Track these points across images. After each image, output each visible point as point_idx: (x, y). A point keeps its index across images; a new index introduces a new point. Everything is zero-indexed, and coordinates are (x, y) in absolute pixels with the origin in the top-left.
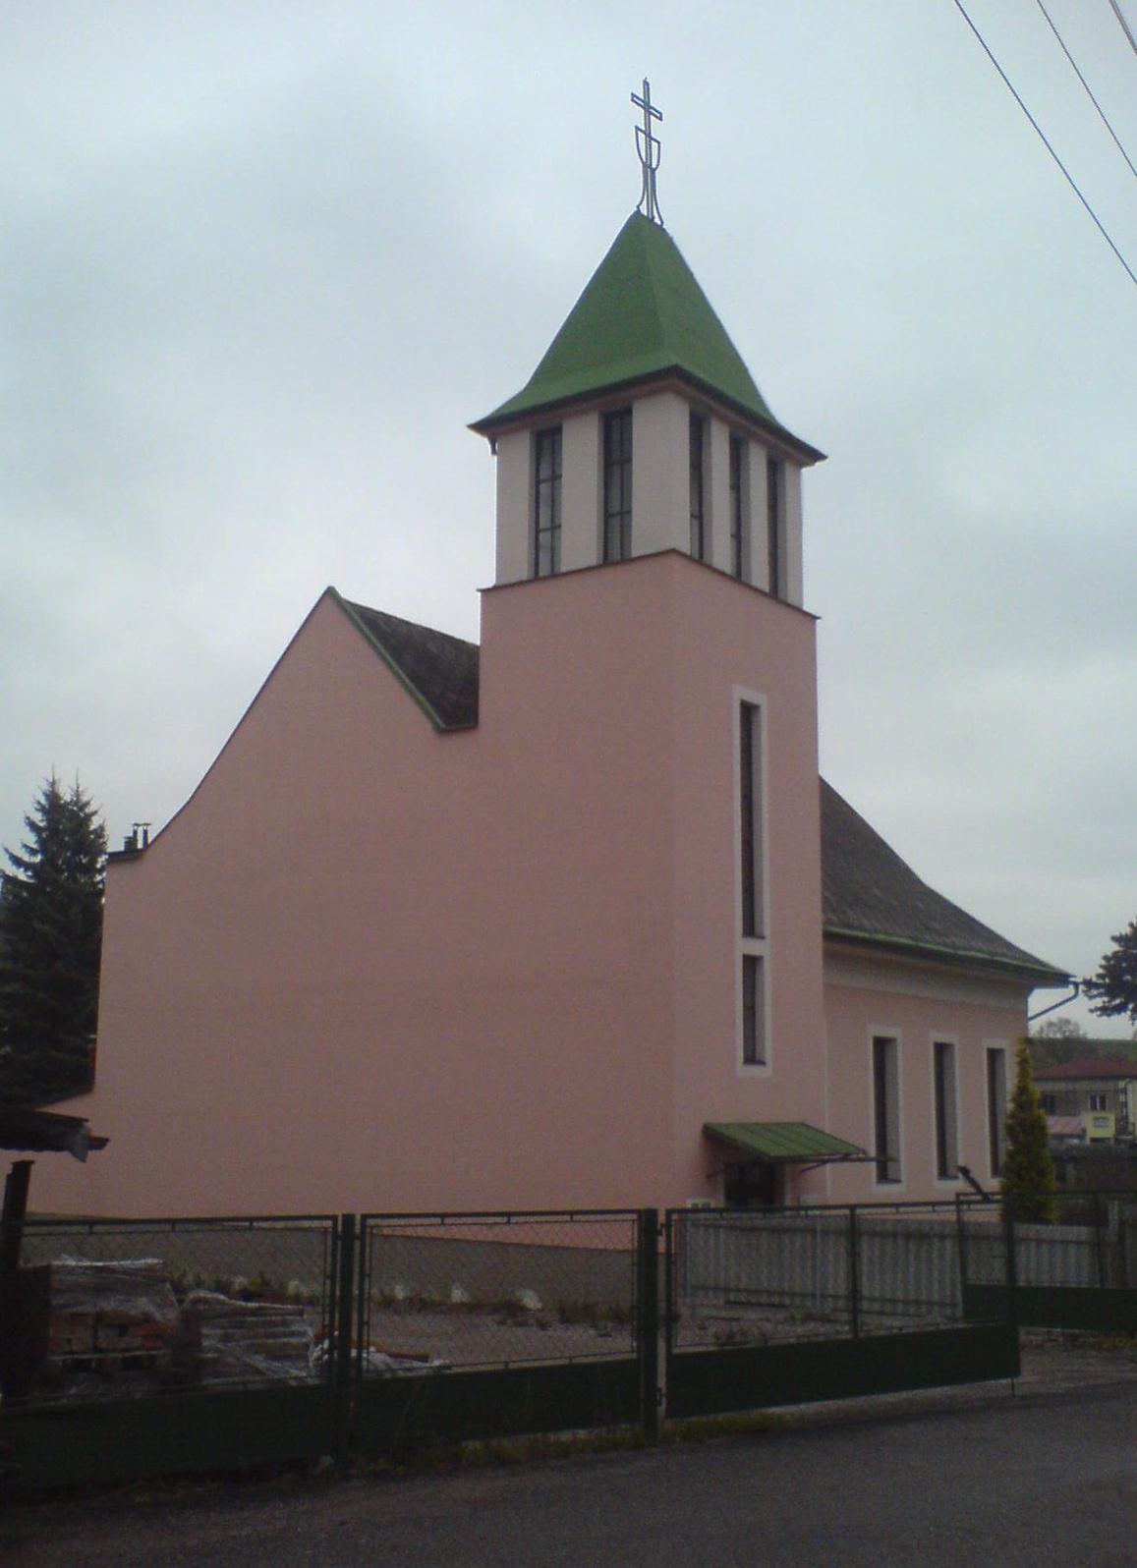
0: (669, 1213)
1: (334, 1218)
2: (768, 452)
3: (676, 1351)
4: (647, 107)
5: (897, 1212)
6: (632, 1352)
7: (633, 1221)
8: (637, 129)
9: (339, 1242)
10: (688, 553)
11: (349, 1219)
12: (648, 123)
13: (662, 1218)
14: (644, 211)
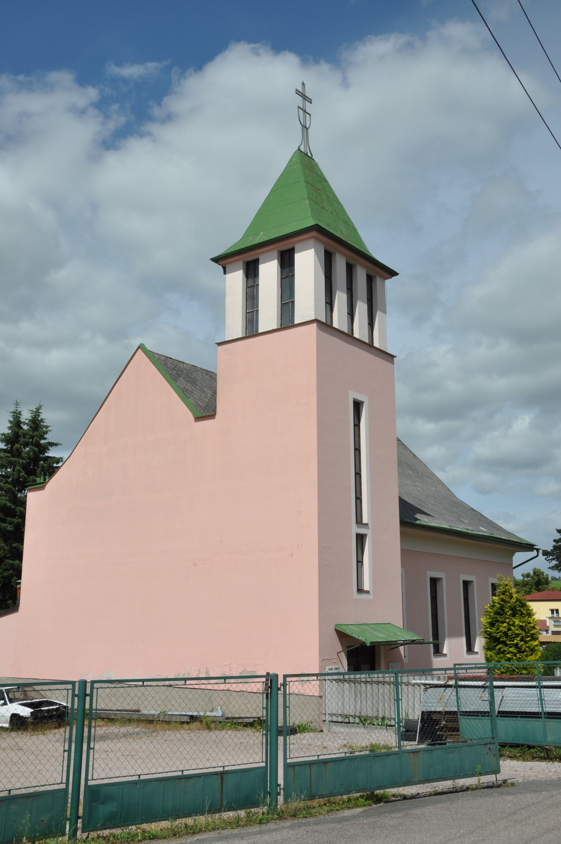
0: (285, 676)
1: (73, 683)
2: (367, 272)
3: (289, 761)
4: (304, 97)
5: (185, 684)
6: (263, 762)
7: (263, 682)
8: (299, 107)
9: (76, 698)
10: (324, 321)
11: (84, 683)
12: (304, 105)
13: (281, 681)
14: (302, 149)
